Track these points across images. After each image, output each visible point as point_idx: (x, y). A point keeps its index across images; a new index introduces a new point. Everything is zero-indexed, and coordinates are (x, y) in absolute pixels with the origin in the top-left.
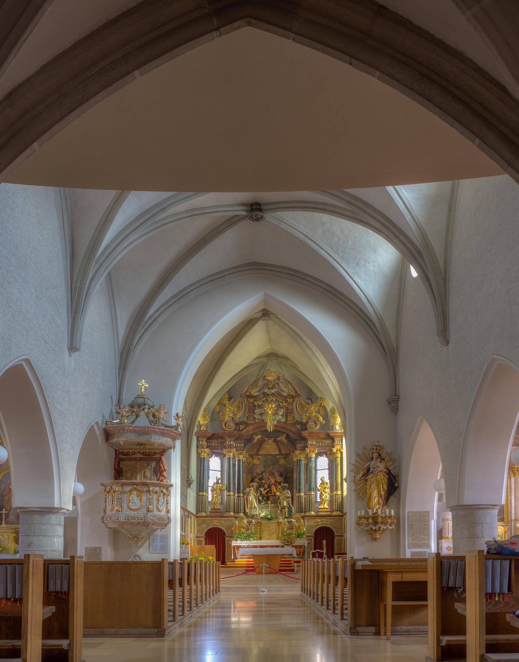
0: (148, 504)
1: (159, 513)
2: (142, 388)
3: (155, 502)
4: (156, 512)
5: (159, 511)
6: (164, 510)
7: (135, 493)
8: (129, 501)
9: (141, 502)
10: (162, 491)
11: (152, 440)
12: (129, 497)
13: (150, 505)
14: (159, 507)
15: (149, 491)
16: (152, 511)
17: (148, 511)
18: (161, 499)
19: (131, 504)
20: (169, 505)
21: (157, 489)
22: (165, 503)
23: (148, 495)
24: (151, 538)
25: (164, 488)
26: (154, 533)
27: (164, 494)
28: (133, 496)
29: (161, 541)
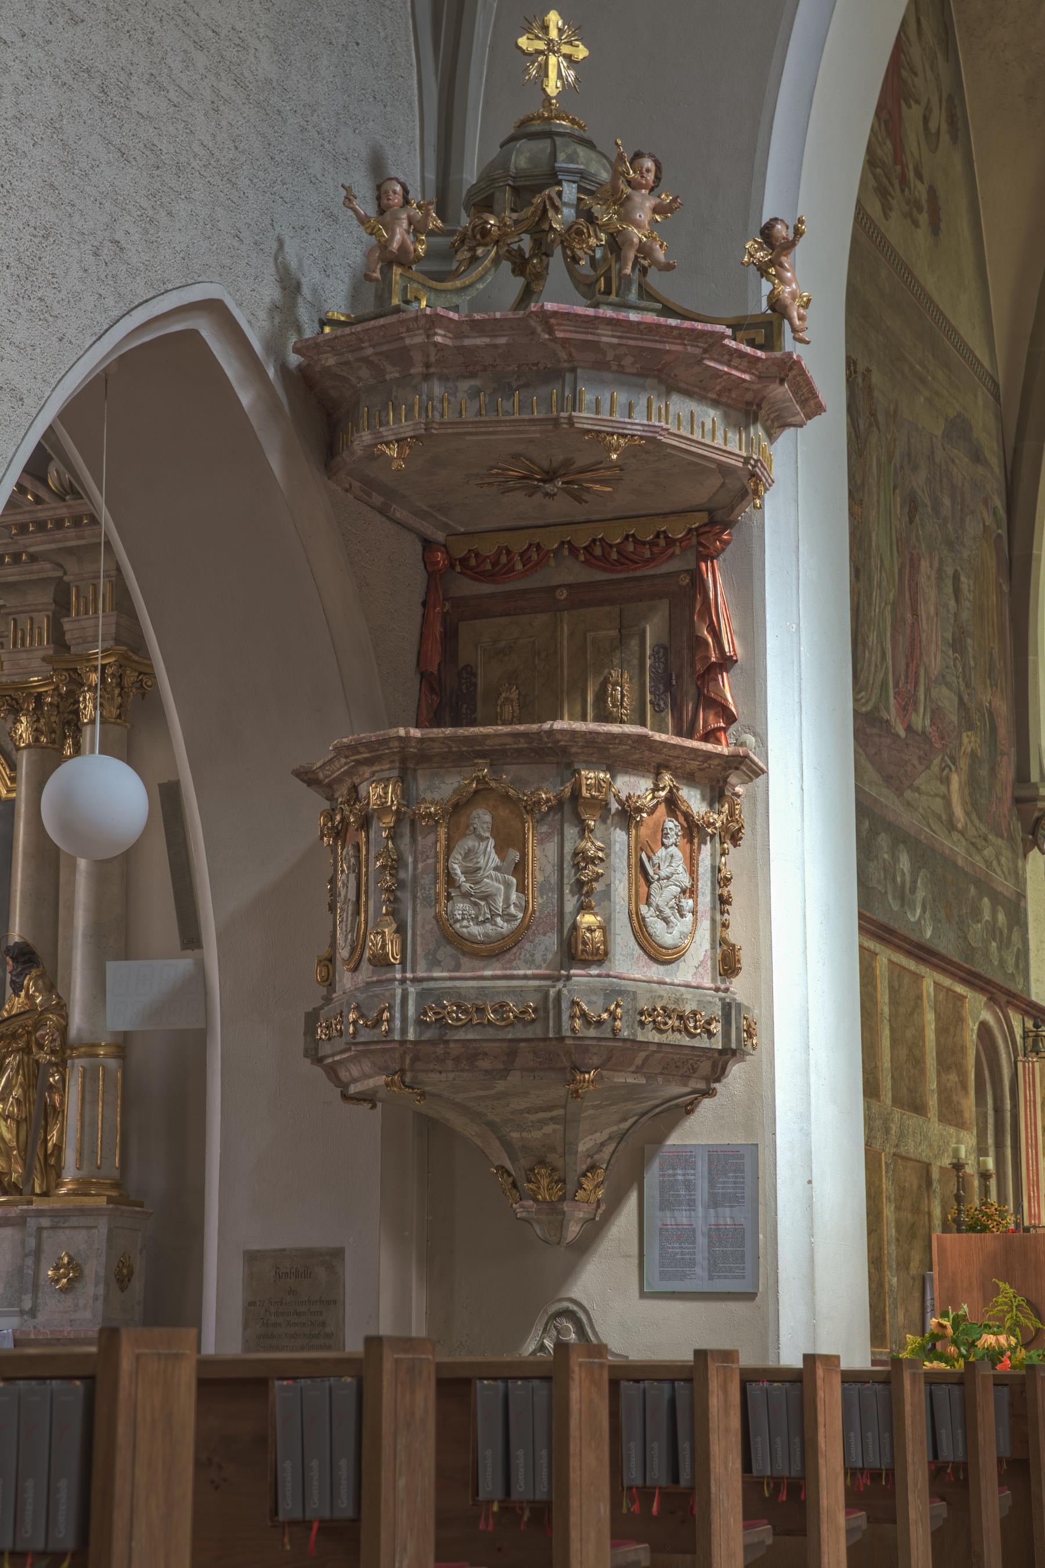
0: (570, 903)
1: (655, 972)
2: (544, 69)
3: (621, 888)
4: (628, 964)
5: (658, 954)
6: (701, 948)
7: (482, 818)
8: (450, 880)
9: (522, 888)
10: (672, 804)
11: (585, 417)
12: (449, 850)
13: (584, 908)
14: (657, 927)
15: (576, 794)
16: (600, 957)
17: (574, 952)
18: (670, 861)
19: (461, 908)
20: (736, 914)
21: (635, 786)
22: (705, 899)
23: (571, 832)
24: (652, 1176)
25: (690, 779)
26: (674, 1140)
27: (693, 831)
28: (470, 842)
29: (714, 1202)
